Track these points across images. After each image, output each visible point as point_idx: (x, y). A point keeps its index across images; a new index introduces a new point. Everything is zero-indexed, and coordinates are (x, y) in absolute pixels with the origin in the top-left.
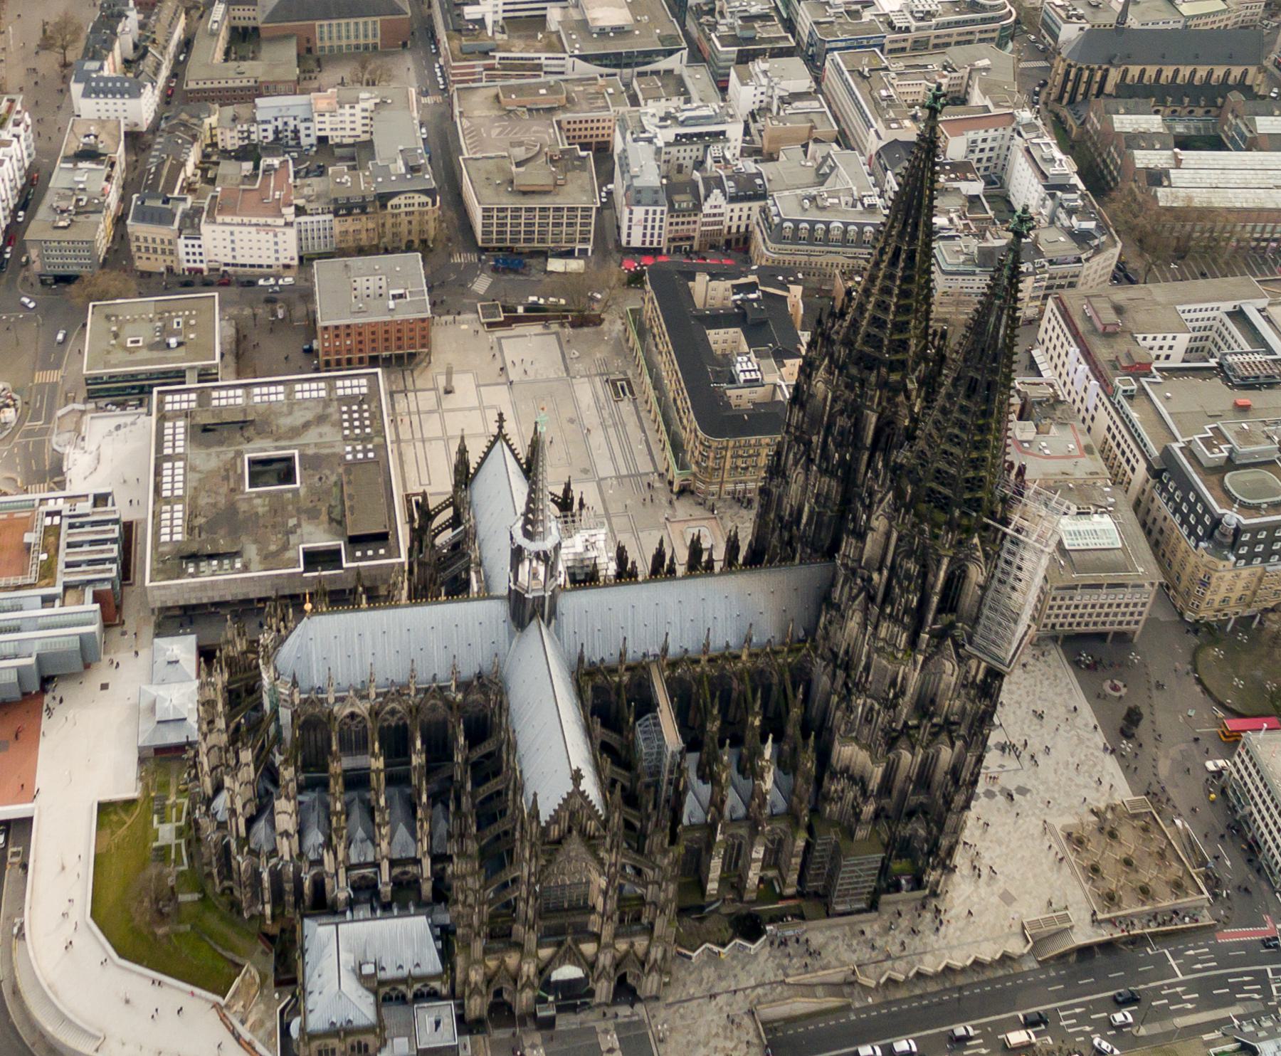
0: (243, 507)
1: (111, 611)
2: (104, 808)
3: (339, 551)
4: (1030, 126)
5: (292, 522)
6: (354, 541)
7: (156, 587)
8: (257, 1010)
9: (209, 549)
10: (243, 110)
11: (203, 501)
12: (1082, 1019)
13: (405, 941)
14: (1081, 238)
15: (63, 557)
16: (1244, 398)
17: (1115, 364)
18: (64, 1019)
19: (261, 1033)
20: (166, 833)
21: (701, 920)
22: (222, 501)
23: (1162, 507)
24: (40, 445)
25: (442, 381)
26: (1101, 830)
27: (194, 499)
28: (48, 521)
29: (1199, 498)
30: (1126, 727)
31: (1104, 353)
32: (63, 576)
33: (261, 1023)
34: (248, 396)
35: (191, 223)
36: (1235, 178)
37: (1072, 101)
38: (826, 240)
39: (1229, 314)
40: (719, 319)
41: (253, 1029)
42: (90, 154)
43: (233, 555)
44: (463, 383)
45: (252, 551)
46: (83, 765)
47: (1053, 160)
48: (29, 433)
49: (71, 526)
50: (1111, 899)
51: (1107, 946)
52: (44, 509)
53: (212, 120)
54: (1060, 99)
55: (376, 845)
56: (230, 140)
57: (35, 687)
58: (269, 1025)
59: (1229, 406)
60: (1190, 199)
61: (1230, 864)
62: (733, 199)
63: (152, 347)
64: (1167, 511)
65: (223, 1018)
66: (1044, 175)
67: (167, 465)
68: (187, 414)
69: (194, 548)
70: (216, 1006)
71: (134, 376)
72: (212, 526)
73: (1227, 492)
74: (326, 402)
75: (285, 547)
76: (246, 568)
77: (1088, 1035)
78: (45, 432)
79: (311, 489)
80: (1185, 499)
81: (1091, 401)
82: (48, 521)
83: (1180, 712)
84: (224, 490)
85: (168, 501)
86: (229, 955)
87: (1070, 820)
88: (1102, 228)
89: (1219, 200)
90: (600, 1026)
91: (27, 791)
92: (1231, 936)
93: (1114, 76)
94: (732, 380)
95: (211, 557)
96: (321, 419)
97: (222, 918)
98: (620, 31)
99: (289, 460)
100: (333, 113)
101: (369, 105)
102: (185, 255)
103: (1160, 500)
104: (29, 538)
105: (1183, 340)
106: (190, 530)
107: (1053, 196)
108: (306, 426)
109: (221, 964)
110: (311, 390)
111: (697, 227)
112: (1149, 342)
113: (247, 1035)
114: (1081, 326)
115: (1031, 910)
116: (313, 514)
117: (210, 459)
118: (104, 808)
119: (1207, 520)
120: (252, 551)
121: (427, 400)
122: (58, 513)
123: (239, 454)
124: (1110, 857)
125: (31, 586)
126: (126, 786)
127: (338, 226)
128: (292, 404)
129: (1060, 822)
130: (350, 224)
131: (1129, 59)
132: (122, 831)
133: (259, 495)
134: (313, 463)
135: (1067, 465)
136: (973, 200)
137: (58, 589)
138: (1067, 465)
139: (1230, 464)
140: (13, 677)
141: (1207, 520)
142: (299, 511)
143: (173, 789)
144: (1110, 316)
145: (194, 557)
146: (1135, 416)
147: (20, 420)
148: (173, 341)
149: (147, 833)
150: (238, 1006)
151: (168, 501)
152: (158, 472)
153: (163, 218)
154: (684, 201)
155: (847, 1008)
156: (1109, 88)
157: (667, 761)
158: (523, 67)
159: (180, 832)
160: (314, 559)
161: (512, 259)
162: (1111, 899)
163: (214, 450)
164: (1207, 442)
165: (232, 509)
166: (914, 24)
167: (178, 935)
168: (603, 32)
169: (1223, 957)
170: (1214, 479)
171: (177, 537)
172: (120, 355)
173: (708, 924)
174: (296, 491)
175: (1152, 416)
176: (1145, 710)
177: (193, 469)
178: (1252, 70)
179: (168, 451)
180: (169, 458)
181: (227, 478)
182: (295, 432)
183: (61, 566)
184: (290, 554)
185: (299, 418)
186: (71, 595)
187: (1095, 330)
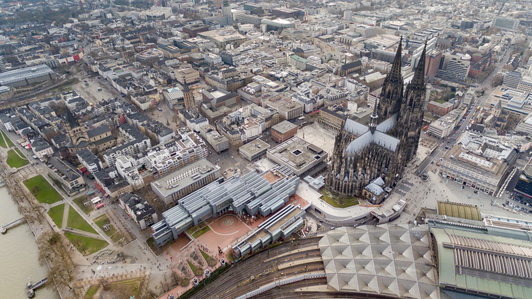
14: (365, 88)
15: (283, 173)
20: (331, 196)
56: (229, 122)
98: (278, 86)
102: (243, 138)
111: (316, 105)
120: (307, 161)
145: (300, 165)
168: (275, 87)
172: (253, 152)
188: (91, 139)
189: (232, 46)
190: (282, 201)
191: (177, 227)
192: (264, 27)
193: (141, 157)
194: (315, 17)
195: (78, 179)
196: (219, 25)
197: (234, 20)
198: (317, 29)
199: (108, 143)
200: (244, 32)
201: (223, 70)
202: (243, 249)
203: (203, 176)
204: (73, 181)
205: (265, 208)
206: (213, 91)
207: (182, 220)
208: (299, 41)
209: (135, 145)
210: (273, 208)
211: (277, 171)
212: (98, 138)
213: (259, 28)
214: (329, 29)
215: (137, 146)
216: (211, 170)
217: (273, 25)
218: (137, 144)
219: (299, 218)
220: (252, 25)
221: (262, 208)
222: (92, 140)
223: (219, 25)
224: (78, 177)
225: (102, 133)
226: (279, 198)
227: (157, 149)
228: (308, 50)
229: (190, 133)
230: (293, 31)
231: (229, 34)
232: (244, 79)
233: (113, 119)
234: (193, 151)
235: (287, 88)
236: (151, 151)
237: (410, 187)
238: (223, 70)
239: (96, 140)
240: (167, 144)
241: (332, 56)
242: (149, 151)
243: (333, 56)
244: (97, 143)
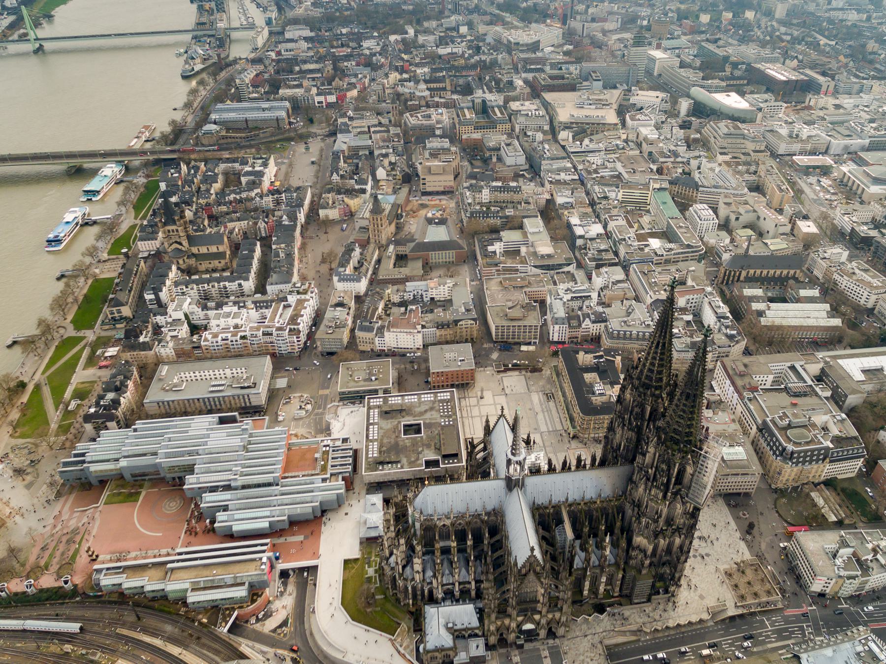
0: (401, 443)
1: (349, 484)
2: (346, 562)
3: (438, 461)
4: (711, 294)
5: (420, 449)
6: (445, 457)
7: (367, 475)
8: (407, 642)
9: (388, 460)
10: (401, 287)
11: (385, 441)
12: (731, 645)
13: (464, 614)
15: (330, 463)
16: (795, 400)
17: (744, 387)
18: (330, 645)
19: (408, 650)
20: (371, 572)
21: (581, 606)
22: (393, 441)
23: (763, 443)
24: (321, 419)
25: (479, 394)
26: (739, 570)
27: (381, 440)
28: (324, 449)
29: (777, 440)
30: (749, 530)
31: (739, 382)
32: (330, 471)
33: (408, 646)
34: (403, 400)
35: (380, 331)
36: (791, 314)
37: (727, 283)
38: (630, 338)
39: (789, 367)
40: (588, 369)
41: (405, 649)
42: (341, 304)
43: (397, 462)
44: (488, 395)
45: (404, 461)
46: (337, 546)
47: (719, 307)
48: (317, 414)
49: (333, 451)
50: (742, 597)
51: (741, 616)
52: (322, 444)
53: (389, 291)
54: (722, 283)
55: (453, 576)
56: (396, 299)
57: (319, 514)
58: (411, 647)
59: (789, 404)
60: (774, 322)
61: (789, 584)
62: (594, 322)
63: (365, 380)
64: (765, 445)
65: (393, 644)
66: (716, 313)
67: (371, 427)
68: (379, 407)
69: (382, 459)
70: (390, 639)
71: (358, 392)
72: (389, 451)
73: (788, 437)
74: (434, 402)
75: (418, 459)
76: (402, 467)
77: (733, 651)
78: (323, 414)
79: (428, 436)
80: (771, 440)
81: (735, 401)
82: (324, 449)
83: (769, 525)
84: (393, 436)
85: (371, 441)
86: (395, 619)
87: (727, 566)
88: (739, 333)
89: (785, 323)
90: (541, 647)
91: (316, 555)
92: (790, 612)
93: (744, 274)
94: (594, 393)
95: (388, 463)
96: (432, 409)
97: (393, 605)
98: (549, 256)
99: (419, 425)
100: (436, 288)
101: (451, 285)
103: (762, 441)
104: (317, 455)
105: (771, 378)
106: (380, 452)
107: (720, 321)
108: (426, 411)
109: (392, 623)
110: (428, 397)
111: (580, 333)
112: (758, 378)
113: (402, 651)
114: (731, 372)
115: (711, 602)
116: (428, 446)
117: (388, 424)
118: (346, 562)
119: (780, 448)
120: (404, 461)
121: (473, 401)
122: (328, 446)
123: (399, 422)
124: (742, 581)
125: (317, 474)
126: (355, 553)
127: (438, 333)
128: (420, 403)
129: (723, 567)
130: (443, 332)
131: (749, 267)
132: (353, 571)
133: (407, 439)
134: (428, 426)
135: (725, 427)
136: (688, 322)
137: (328, 476)
138: (725, 427)
139: (789, 426)
140: (310, 510)
141: (780, 448)
142: (423, 445)
143: (373, 554)
144: (742, 368)
145: (382, 463)
146: (752, 407)
147: (313, 409)
148: (373, 378)
149: (363, 571)
150: (399, 640)
151: (371, 441)
152: (368, 430)
153: (369, 329)
154: (574, 323)
155: (639, 640)
156: (742, 278)
157: (568, 543)
158: (511, 270)
159: (376, 571)
160: (429, 464)
161: (507, 346)
162: (742, 597)
163: (389, 421)
164: (780, 417)
165: (397, 444)
166: (665, 253)
167: (375, 612)
168: (542, 256)
169: (787, 620)
170: (783, 432)
171: (375, 455)
172: (352, 384)
173: (584, 607)
174: (422, 437)
175: (759, 408)
176: (756, 523)
177: (381, 428)
178: (798, 271)
179: (371, 421)
180: (372, 424)
181: (394, 432)
182: (422, 414)
183: (329, 467)
184: (419, 462)
185: (423, 408)
186: (333, 478)
187: (736, 374)
188: (193, 248)
189: (571, 135)
190: (264, 524)
191: (94, 468)
192: (684, 105)
193: (211, 309)
194: (837, 102)
195: (123, 309)
196: (601, 83)
197: (655, 74)
198: (804, 137)
199: (216, 262)
200: (639, 106)
201: (494, 184)
202: (107, 581)
204: (114, 309)
205: (225, 518)
206: (436, 223)
207: (108, 461)
208: (727, 158)
209: (221, 284)
210: (237, 527)
212: (203, 250)
213: (675, 102)
214: (838, 144)
215: (225, 288)
216: (249, 387)
217: (710, 103)
218: (227, 284)
219: (243, 584)
220: (662, 95)
221: (221, 516)
222: (194, 250)
223: (601, 83)
224: (123, 305)
225: (211, 244)
226: (268, 514)
227: (242, 305)
228: (715, 187)
229: (303, 297)
230: (726, 130)
231: (593, 107)
232: (507, 217)
233: (256, 224)
234: (271, 334)
235: (569, 265)
236: (231, 304)
238: (494, 184)
239: (201, 252)
240: (260, 302)
241: (758, 218)
242: (226, 303)
243: (762, 219)
244: (198, 257)
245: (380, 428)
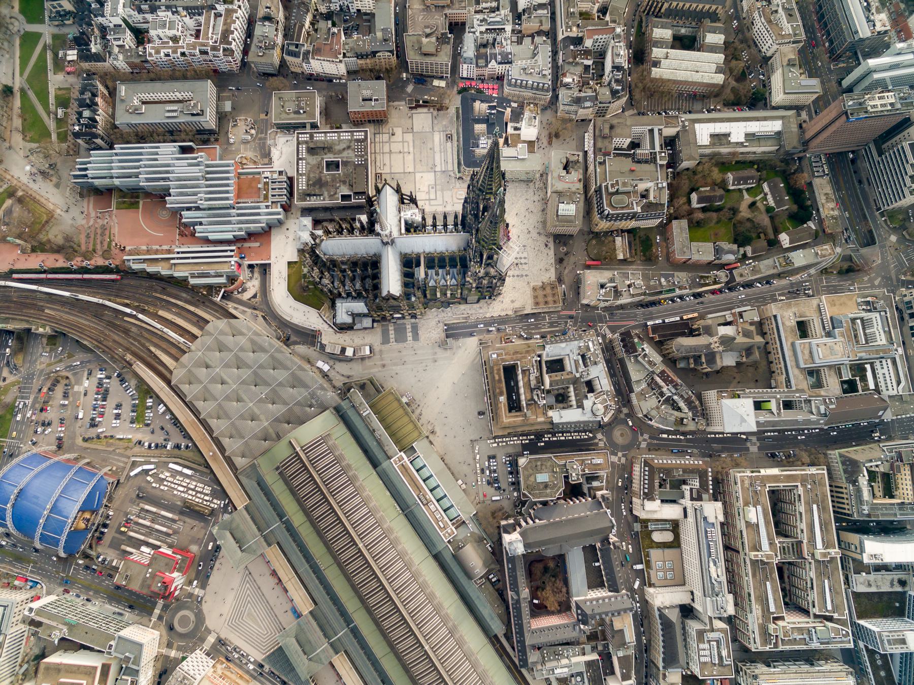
0: (323, 179)
68: (306, 142)
72: (314, 185)
75: (336, 193)
85: (301, 175)
106: (308, 185)
117: (314, 160)
120: (326, 194)
123: (323, 159)
165: (320, 179)
190: (229, 236)
203: (183, 119)
210: (212, 236)
211: (266, 184)
216: (198, 114)
237: (410, 338)
245: (307, 163)
